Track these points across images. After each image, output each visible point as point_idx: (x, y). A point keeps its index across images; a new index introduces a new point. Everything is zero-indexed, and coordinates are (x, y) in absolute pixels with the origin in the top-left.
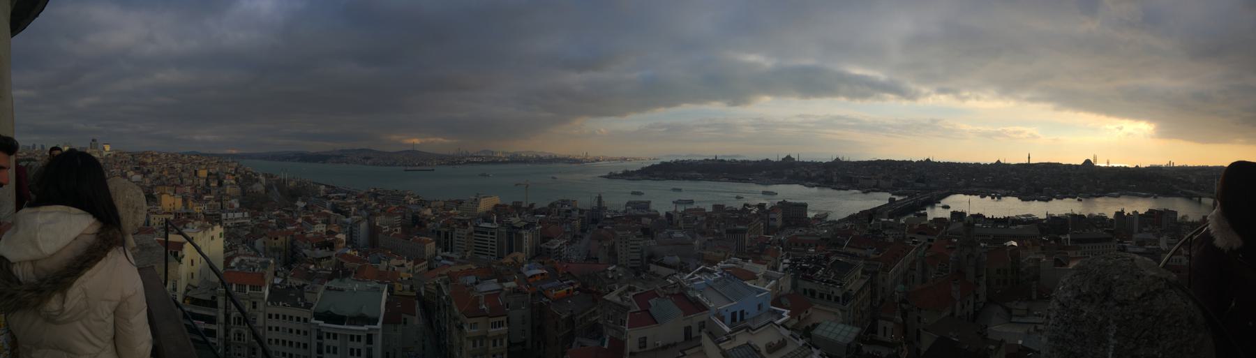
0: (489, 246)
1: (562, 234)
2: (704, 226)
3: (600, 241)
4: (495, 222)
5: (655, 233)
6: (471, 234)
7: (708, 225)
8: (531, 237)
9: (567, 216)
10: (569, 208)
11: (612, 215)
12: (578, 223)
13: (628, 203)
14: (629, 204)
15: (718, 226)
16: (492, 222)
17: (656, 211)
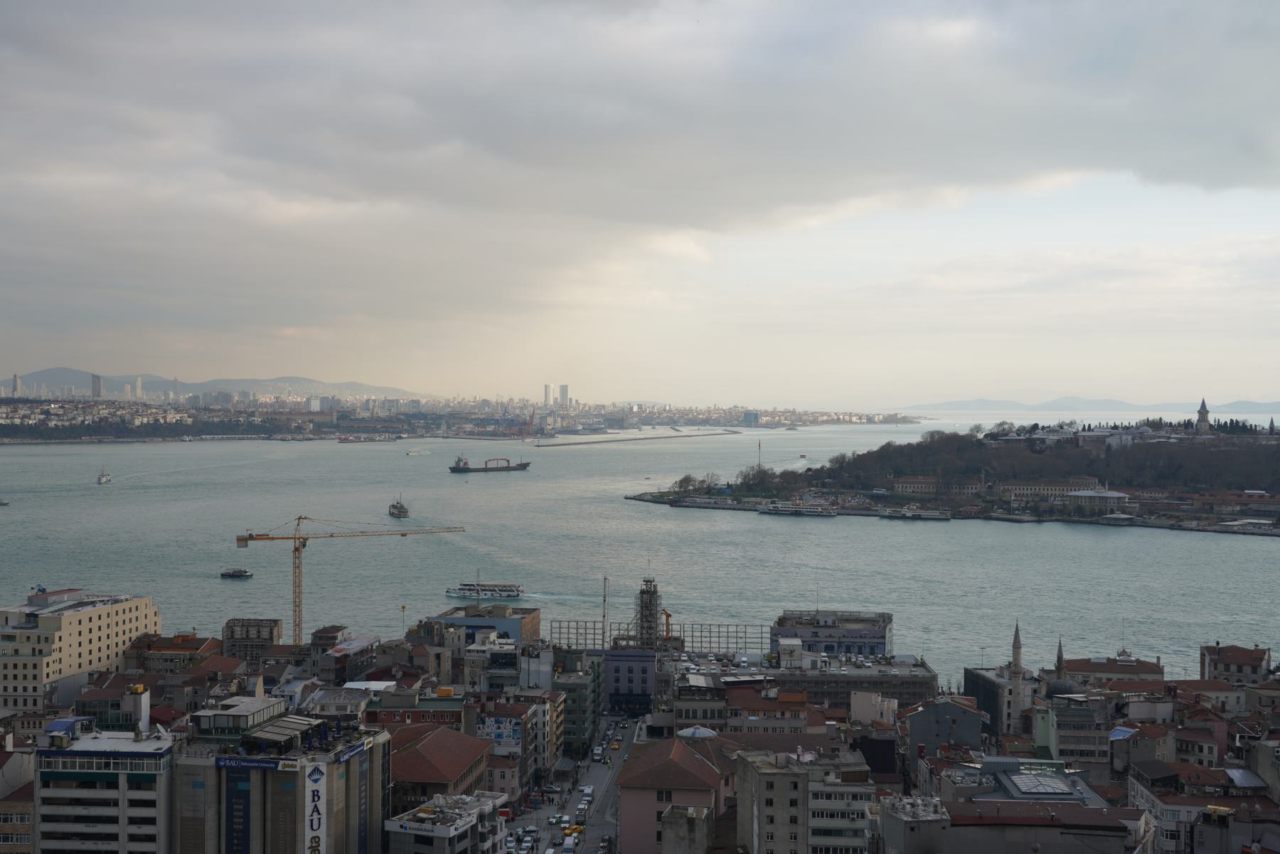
0: (123, 829)
1: (483, 766)
2: (1166, 750)
3: (664, 795)
4: (143, 724)
5: (923, 765)
6: (24, 792)
7: (1183, 748)
8: (340, 784)
9: (496, 686)
10: (508, 646)
11: (714, 676)
12: (547, 716)
13: (781, 621)
14: (785, 624)
15: (1246, 756)
16: (128, 724)
17: (922, 664)
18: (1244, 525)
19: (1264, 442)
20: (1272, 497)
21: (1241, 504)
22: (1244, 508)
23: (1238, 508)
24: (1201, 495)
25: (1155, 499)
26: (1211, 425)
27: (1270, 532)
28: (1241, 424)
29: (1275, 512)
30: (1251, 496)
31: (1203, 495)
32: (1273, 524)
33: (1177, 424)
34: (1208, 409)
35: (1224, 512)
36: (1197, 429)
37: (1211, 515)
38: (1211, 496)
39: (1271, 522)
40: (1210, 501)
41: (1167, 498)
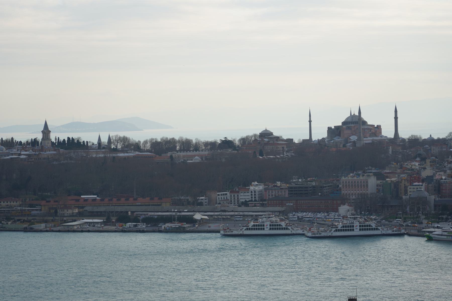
18: (82, 224)
19: (94, 156)
20: (102, 200)
21: (78, 207)
22: (81, 210)
23: (76, 211)
24: (47, 202)
25: (11, 207)
26: (52, 143)
27: (101, 229)
28: (76, 141)
29: (105, 212)
30: (86, 200)
31: (49, 202)
32: (104, 222)
33: (25, 142)
34: (50, 129)
35: (66, 215)
36: (42, 147)
37: (57, 218)
38: (55, 202)
39: (102, 221)
40: (55, 206)
41: (20, 206)
